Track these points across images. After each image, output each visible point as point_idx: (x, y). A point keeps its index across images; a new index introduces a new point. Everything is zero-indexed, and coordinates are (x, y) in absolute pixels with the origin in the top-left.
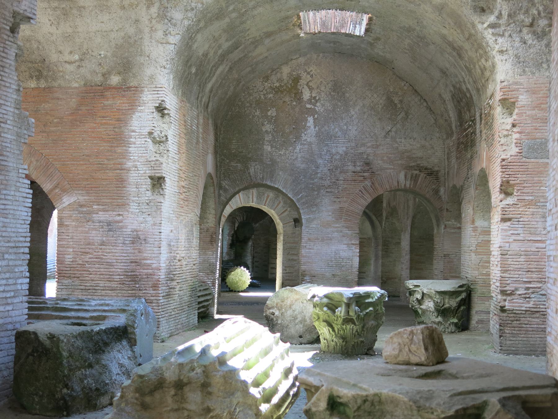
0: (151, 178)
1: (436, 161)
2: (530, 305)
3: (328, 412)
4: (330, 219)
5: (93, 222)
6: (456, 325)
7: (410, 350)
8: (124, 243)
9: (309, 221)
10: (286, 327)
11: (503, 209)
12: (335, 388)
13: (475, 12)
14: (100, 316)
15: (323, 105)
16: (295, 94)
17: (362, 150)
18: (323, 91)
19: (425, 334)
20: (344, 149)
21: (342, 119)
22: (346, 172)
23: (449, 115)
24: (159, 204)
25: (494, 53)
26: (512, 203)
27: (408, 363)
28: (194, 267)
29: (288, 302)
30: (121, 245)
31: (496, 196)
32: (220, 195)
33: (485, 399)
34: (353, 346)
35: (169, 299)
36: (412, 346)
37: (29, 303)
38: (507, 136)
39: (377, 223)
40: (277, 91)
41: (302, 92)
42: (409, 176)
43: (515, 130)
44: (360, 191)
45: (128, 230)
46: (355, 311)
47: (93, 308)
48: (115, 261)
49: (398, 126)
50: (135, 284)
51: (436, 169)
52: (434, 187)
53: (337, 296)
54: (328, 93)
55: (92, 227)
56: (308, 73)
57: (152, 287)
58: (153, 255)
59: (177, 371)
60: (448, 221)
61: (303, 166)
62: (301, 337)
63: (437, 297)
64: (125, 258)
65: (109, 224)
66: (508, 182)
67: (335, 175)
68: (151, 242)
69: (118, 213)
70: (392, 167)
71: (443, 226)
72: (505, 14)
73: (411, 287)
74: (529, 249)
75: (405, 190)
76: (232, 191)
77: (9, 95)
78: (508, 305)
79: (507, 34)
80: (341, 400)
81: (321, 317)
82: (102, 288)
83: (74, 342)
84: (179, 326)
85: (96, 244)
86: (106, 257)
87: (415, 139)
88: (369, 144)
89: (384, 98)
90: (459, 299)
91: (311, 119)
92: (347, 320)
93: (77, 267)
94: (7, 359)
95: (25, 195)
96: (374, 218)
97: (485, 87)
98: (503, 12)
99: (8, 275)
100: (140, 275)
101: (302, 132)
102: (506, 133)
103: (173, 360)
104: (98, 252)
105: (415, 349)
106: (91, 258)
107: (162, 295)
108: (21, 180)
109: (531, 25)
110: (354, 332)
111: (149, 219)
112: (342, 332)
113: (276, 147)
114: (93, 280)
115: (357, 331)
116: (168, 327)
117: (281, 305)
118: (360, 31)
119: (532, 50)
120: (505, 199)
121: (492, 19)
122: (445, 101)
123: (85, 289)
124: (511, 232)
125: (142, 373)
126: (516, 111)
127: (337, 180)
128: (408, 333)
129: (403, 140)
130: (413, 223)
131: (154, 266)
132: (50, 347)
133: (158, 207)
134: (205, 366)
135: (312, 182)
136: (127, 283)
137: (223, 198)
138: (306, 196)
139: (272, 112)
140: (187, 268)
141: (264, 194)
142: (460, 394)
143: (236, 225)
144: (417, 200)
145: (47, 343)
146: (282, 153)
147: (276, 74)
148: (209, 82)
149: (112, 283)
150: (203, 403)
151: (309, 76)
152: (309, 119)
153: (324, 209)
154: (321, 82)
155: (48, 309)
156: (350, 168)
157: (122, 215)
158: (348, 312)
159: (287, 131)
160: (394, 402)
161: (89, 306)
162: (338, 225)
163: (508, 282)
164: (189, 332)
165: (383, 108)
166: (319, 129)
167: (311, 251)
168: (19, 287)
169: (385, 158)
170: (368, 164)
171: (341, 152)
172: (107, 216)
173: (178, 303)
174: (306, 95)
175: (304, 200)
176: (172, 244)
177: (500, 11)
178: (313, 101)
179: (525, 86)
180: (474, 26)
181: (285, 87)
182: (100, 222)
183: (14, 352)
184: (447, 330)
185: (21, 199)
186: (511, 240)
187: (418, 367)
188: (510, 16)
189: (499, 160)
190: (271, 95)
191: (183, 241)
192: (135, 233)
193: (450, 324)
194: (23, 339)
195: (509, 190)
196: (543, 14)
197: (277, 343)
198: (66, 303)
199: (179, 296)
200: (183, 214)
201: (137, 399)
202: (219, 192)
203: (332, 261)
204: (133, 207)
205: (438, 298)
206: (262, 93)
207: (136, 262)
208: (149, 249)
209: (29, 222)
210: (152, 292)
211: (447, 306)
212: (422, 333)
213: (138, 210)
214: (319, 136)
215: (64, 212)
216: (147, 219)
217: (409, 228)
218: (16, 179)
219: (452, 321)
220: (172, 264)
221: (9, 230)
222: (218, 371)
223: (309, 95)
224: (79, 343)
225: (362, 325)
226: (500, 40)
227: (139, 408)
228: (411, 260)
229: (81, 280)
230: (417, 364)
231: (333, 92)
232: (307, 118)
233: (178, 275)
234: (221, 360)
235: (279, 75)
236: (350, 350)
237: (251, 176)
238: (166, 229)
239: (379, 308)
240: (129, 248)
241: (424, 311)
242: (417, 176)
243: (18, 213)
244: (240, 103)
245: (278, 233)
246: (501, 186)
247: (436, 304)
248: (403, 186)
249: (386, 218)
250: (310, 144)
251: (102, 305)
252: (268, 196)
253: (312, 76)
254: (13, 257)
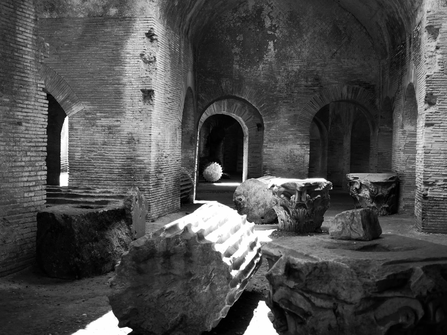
0: (143, 91)
1: (373, 77)
3: (285, 277)
4: (286, 124)
5: (97, 127)
6: (387, 209)
7: (351, 228)
8: (121, 144)
9: (270, 126)
10: (251, 210)
12: (292, 257)
14: (103, 201)
15: (281, 32)
16: (259, 23)
18: (282, 20)
19: (364, 215)
20: (298, 67)
21: (297, 43)
22: (300, 86)
23: (384, 40)
24: (149, 112)
26: (434, 111)
27: (349, 239)
28: (178, 163)
29: (253, 191)
30: (119, 145)
31: (421, 105)
32: (198, 105)
33: (411, 267)
34: (305, 225)
35: (158, 188)
36: (353, 225)
37: (47, 190)
38: (431, 56)
39: (324, 127)
40: (244, 20)
41: (264, 21)
43: (438, 51)
44: (311, 101)
45: (125, 133)
46: (306, 198)
47: (98, 195)
48: (114, 158)
49: (342, 48)
50: (131, 176)
51: (373, 83)
52: (371, 98)
53: (292, 186)
54: (285, 22)
55: (96, 130)
56: (269, 6)
57: (144, 178)
58: (145, 153)
59: (165, 244)
60: (382, 126)
61: (265, 81)
62: (262, 218)
63: (372, 187)
64: (123, 155)
65: (110, 128)
66: (431, 94)
68: (143, 143)
69: (117, 119)
70: (337, 82)
71: (378, 130)
73: (351, 179)
75: (347, 101)
76: (207, 102)
77: (29, 24)
78: (429, 194)
80: (296, 267)
81: (279, 202)
82: (104, 179)
83: (83, 221)
84: (166, 209)
85: (100, 144)
86: (108, 155)
87: (356, 59)
88: (319, 64)
89: (331, 26)
90: (390, 188)
91: (271, 43)
92: (300, 205)
93: (84, 162)
94: (30, 235)
95: (42, 105)
96: (322, 123)
97: (414, 16)
99: (30, 169)
100: (134, 169)
101: (264, 54)
102: (430, 54)
103: (162, 235)
104: (101, 150)
105: (356, 228)
106: (95, 155)
107: (152, 184)
108: (39, 93)
110: (305, 214)
111: (141, 124)
112: (295, 214)
113: (243, 66)
114: (97, 173)
115: (307, 214)
116: (157, 210)
117: (247, 193)
120: (429, 108)
122: (381, 28)
123: (91, 180)
124: (433, 135)
125: (138, 246)
126: (440, 36)
127: (293, 93)
128: (350, 214)
129: (346, 60)
131: (145, 161)
133: (149, 114)
134: (187, 241)
135: (272, 94)
136: (124, 175)
137: (200, 107)
138: (267, 106)
139: (240, 38)
140: (172, 163)
141: (233, 105)
142: (391, 263)
143: (211, 129)
144: (357, 108)
145: (62, 221)
146: (248, 71)
147: (243, 6)
148: (189, 12)
149: (112, 175)
150: (185, 269)
151: (270, 8)
152: (270, 43)
153: (282, 116)
154: (280, 12)
155: (62, 195)
156: (302, 83)
157: (120, 121)
158: (301, 198)
159: (252, 53)
160: (338, 269)
161: (95, 193)
162: (292, 129)
163: (430, 175)
164: (173, 214)
165: (330, 34)
166: (278, 51)
167: (271, 150)
168: (39, 178)
171: (295, 70)
172: (108, 121)
173: (164, 191)
174: (268, 23)
175: (265, 109)
176: (160, 144)
178: (273, 28)
181: (250, 17)
182: (102, 126)
183: (36, 229)
184: (379, 213)
185: (40, 108)
186: (433, 141)
187: (358, 242)
189: (425, 76)
190: (239, 24)
191: (169, 141)
192: (130, 135)
193: (382, 209)
194: (44, 219)
195: (433, 101)
197: (244, 223)
198: (76, 191)
199: (165, 185)
200: (168, 120)
201: (133, 266)
202: (197, 102)
203: (287, 158)
204: (129, 115)
205: (372, 188)
206: (232, 22)
207: (131, 159)
208: (141, 148)
209: (46, 126)
210: (144, 182)
211: (380, 194)
212: (361, 215)
213: (132, 117)
214: (278, 57)
215: (73, 119)
216: (140, 124)
217: (350, 131)
218: (35, 92)
219: (383, 206)
220: (160, 160)
221: (30, 132)
222: (198, 244)
223: (270, 23)
224: (87, 222)
225: (312, 209)
228: (352, 157)
229: (88, 173)
230: (357, 240)
231: (290, 21)
232: (268, 42)
233: (164, 169)
234: (200, 236)
235: (245, 7)
236: (302, 229)
237: (223, 90)
238: (155, 132)
239: (325, 195)
240: (125, 147)
241: (361, 198)
242: (357, 90)
243: (37, 119)
244: (214, 30)
245: (245, 135)
246: (426, 97)
247: (371, 192)
248: (346, 97)
249: (332, 124)
250: (271, 63)
251: (104, 192)
252: (236, 106)
253: (272, 8)
254: (34, 154)
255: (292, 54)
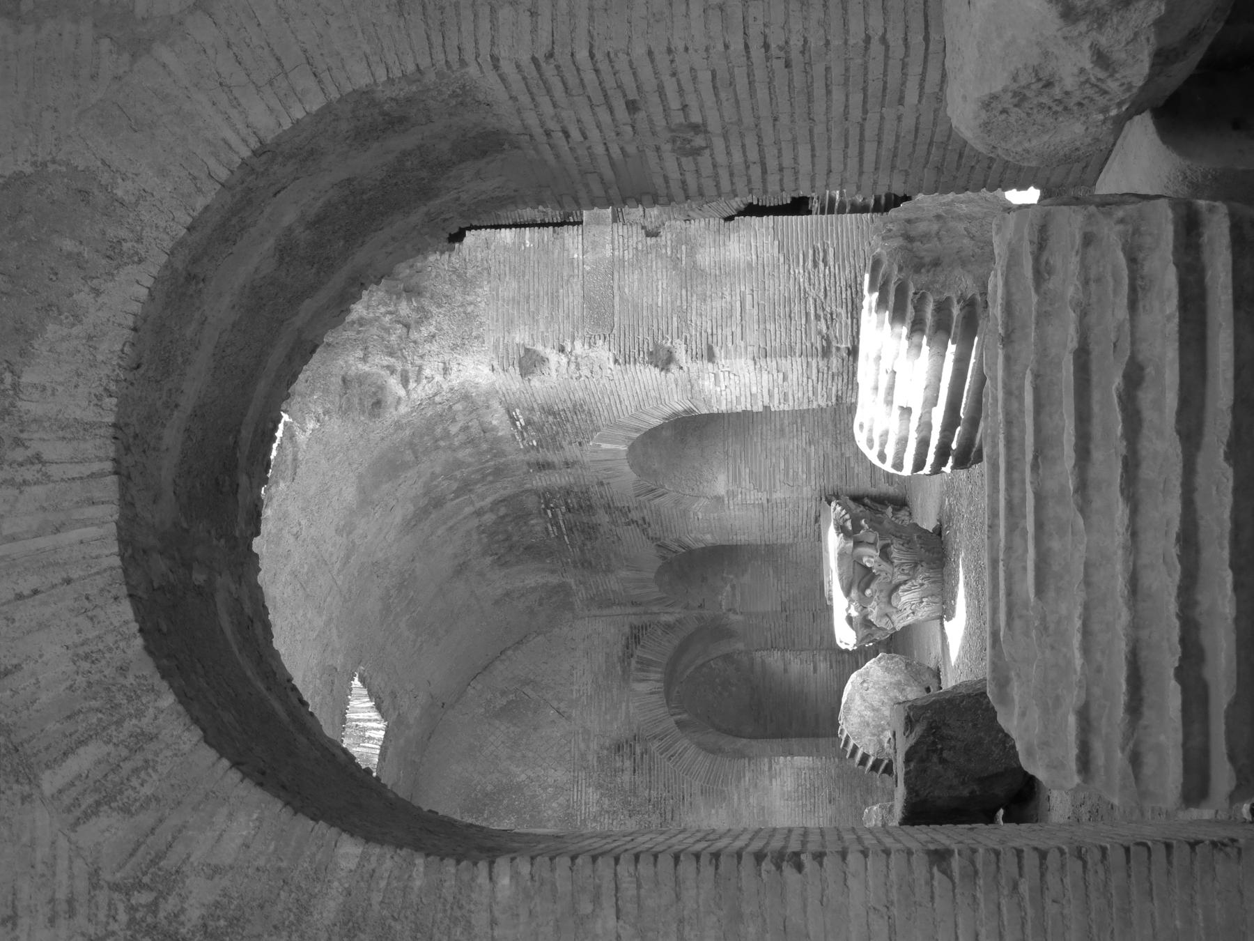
2: (843, 312)
11: (694, 358)
13: (379, 416)
17: (592, 759)
20: (590, 790)
21: (534, 796)
25: (445, 386)
26: (684, 346)
29: (868, 714)
34: (927, 550)
42: (641, 675)
43: (568, 349)
51: (627, 629)
52: (659, 632)
66: (651, 354)
67: (641, 805)
72: (388, 360)
74: (756, 318)
79: (418, 362)
88: (582, 746)
89: (497, 723)
98: (385, 363)
102: (573, 366)
109: (407, 326)
118: (378, 729)
119: (445, 327)
120: (677, 362)
121: (394, 383)
124: (730, 345)
126: (539, 348)
129: (576, 687)
130: (729, 732)
132: (925, 722)
145: (919, 730)
162: (736, 797)
163: (809, 345)
169: (608, 717)
170: (619, 748)
171: (596, 796)
177: (383, 367)
179: (501, 335)
180: (398, 426)
186: (742, 344)
188: (391, 354)
195: (663, 355)
196: (391, 309)
226: (427, 372)
227: (939, 269)
248: (659, 685)
255: (560, 805)
